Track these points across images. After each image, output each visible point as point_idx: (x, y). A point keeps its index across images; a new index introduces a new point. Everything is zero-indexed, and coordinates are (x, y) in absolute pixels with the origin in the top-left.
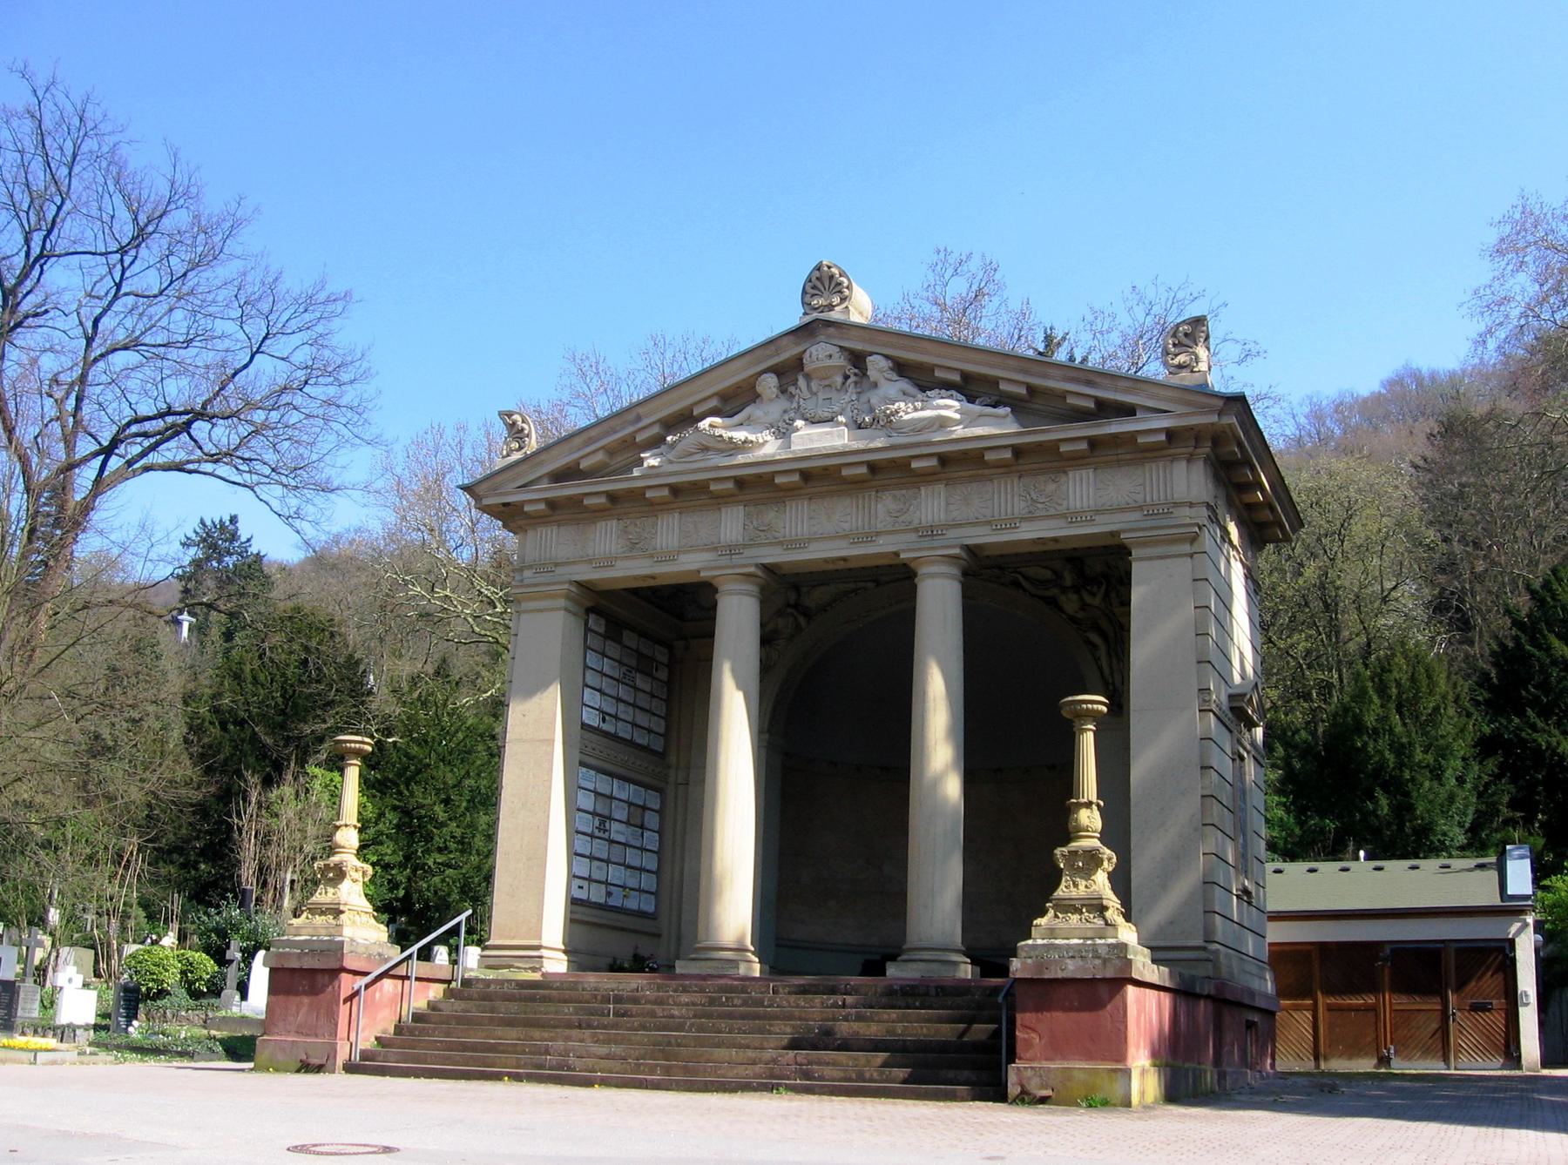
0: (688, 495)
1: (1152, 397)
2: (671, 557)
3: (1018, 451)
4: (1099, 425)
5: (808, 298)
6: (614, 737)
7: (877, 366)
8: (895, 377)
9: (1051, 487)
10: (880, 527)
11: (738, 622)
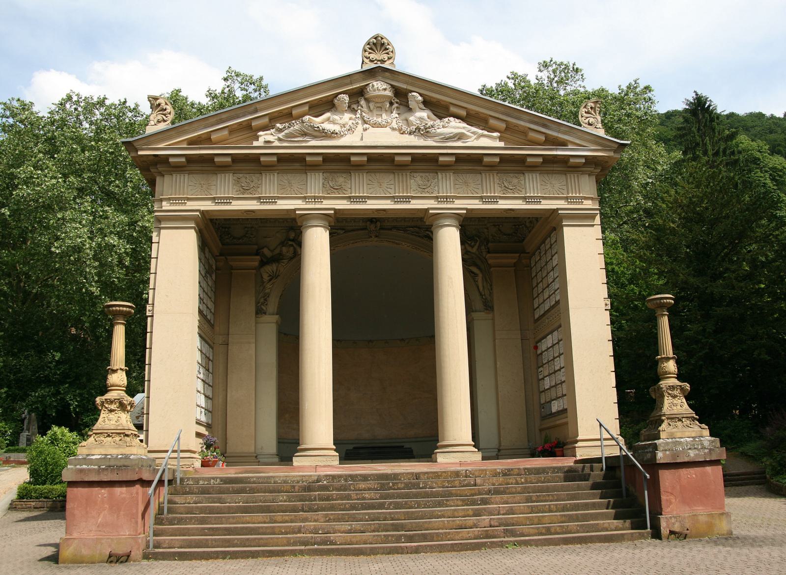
0: (293, 164)
1: (579, 138)
3: (505, 160)
5: (367, 54)
7: (416, 97)
8: (424, 108)
9: (515, 181)
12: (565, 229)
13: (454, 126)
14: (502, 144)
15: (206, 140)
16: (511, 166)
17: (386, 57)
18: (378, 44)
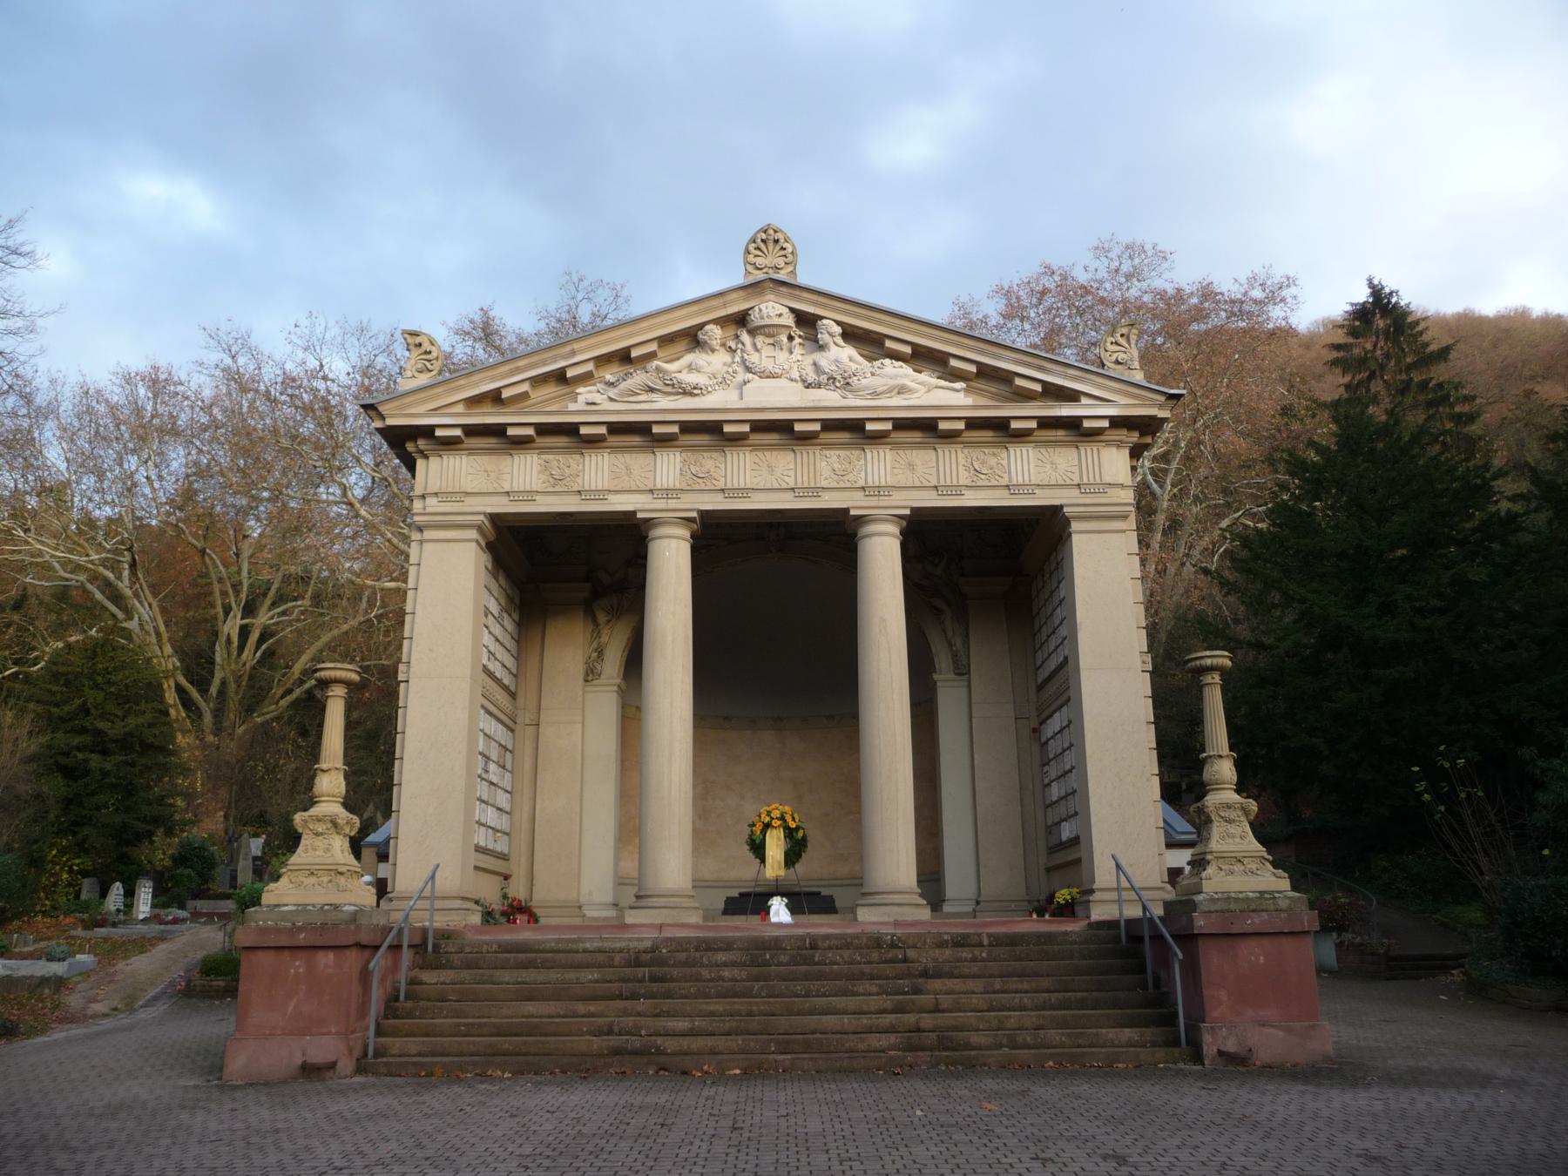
1: (1099, 386)
2: (602, 494)
3: (974, 424)
5: (751, 258)
6: (490, 674)
7: (829, 329)
10: (824, 484)
12: (1075, 537)
14: (969, 401)
15: (495, 397)
17: (781, 262)
18: (768, 239)
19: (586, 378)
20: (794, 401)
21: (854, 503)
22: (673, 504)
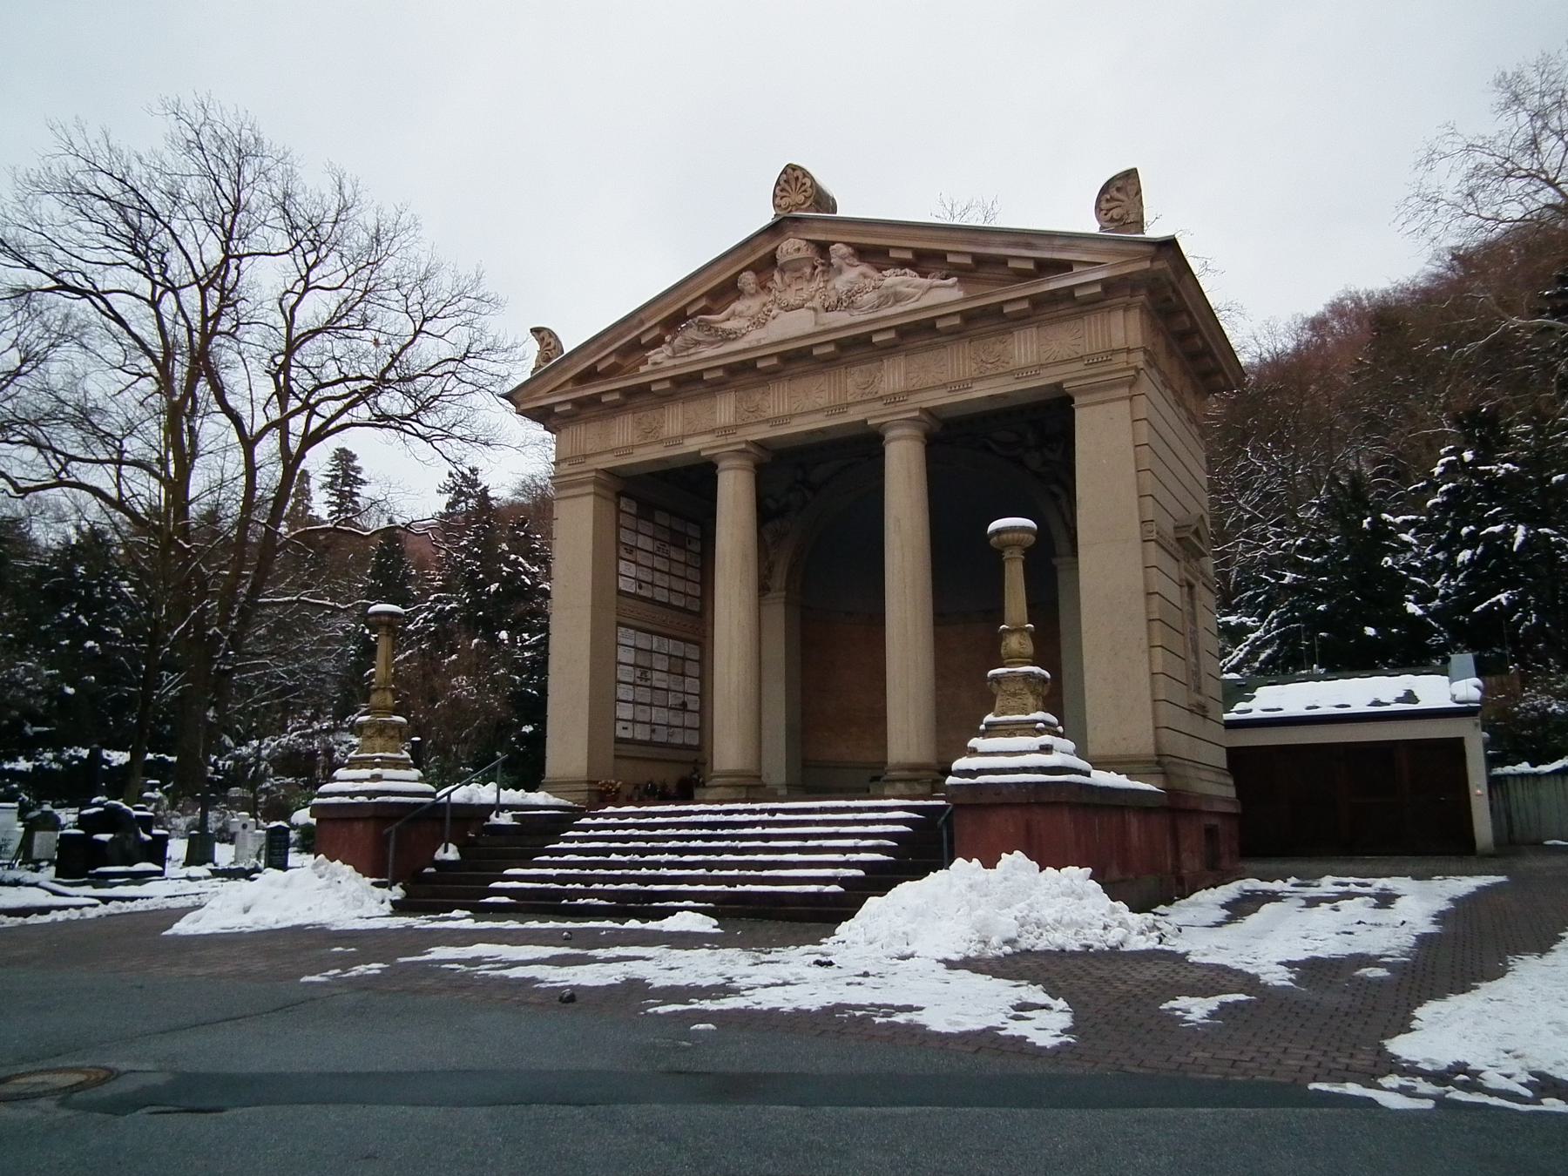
0: (688, 385)
1: (1087, 251)
3: (969, 317)
4: (1039, 284)
6: (652, 601)
7: (839, 250)
10: (850, 399)
11: (734, 497)
12: (1078, 413)
13: (893, 279)
16: (979, 323)
18: (793, 179)
19: (657, 343)
20: (809, 328)
21: (869, 413)
22: (731, 439)
